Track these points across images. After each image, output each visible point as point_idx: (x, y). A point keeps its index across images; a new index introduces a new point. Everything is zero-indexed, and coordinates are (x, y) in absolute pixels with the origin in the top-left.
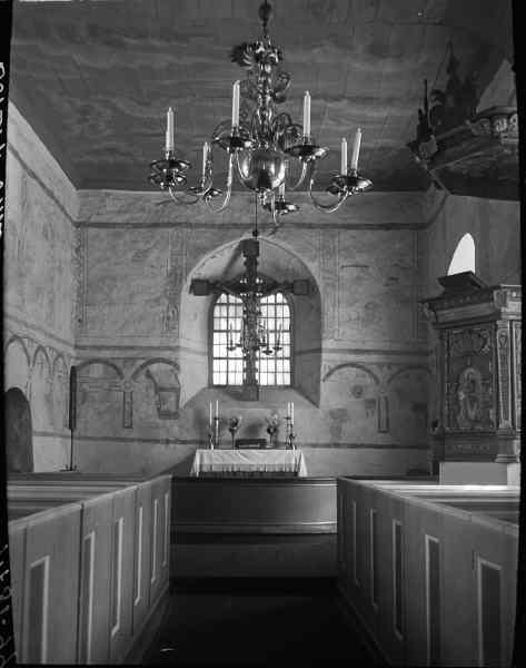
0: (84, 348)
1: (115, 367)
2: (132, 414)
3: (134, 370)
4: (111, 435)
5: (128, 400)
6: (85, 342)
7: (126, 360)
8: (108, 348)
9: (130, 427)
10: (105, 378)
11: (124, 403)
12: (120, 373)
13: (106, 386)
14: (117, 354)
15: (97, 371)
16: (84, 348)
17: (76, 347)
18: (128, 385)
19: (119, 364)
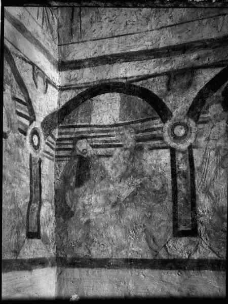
0: (77, 65)
1: (146, 94)
2: (193, 196)
3: (193, 94)
4: (149, 256)
5: (183, 167)
6: (79, 52)
7: (172, 76)
8: (128, 57)
9: (193, 232)
10: (126, 125)
11: (174, 174)
12: (163, 112)
13: (129, 139)
14: (149, 67)
15: (107, 110)
16: (77, 65)
17: (62, 66)
18: (180, 131)
19: (157, 88)
